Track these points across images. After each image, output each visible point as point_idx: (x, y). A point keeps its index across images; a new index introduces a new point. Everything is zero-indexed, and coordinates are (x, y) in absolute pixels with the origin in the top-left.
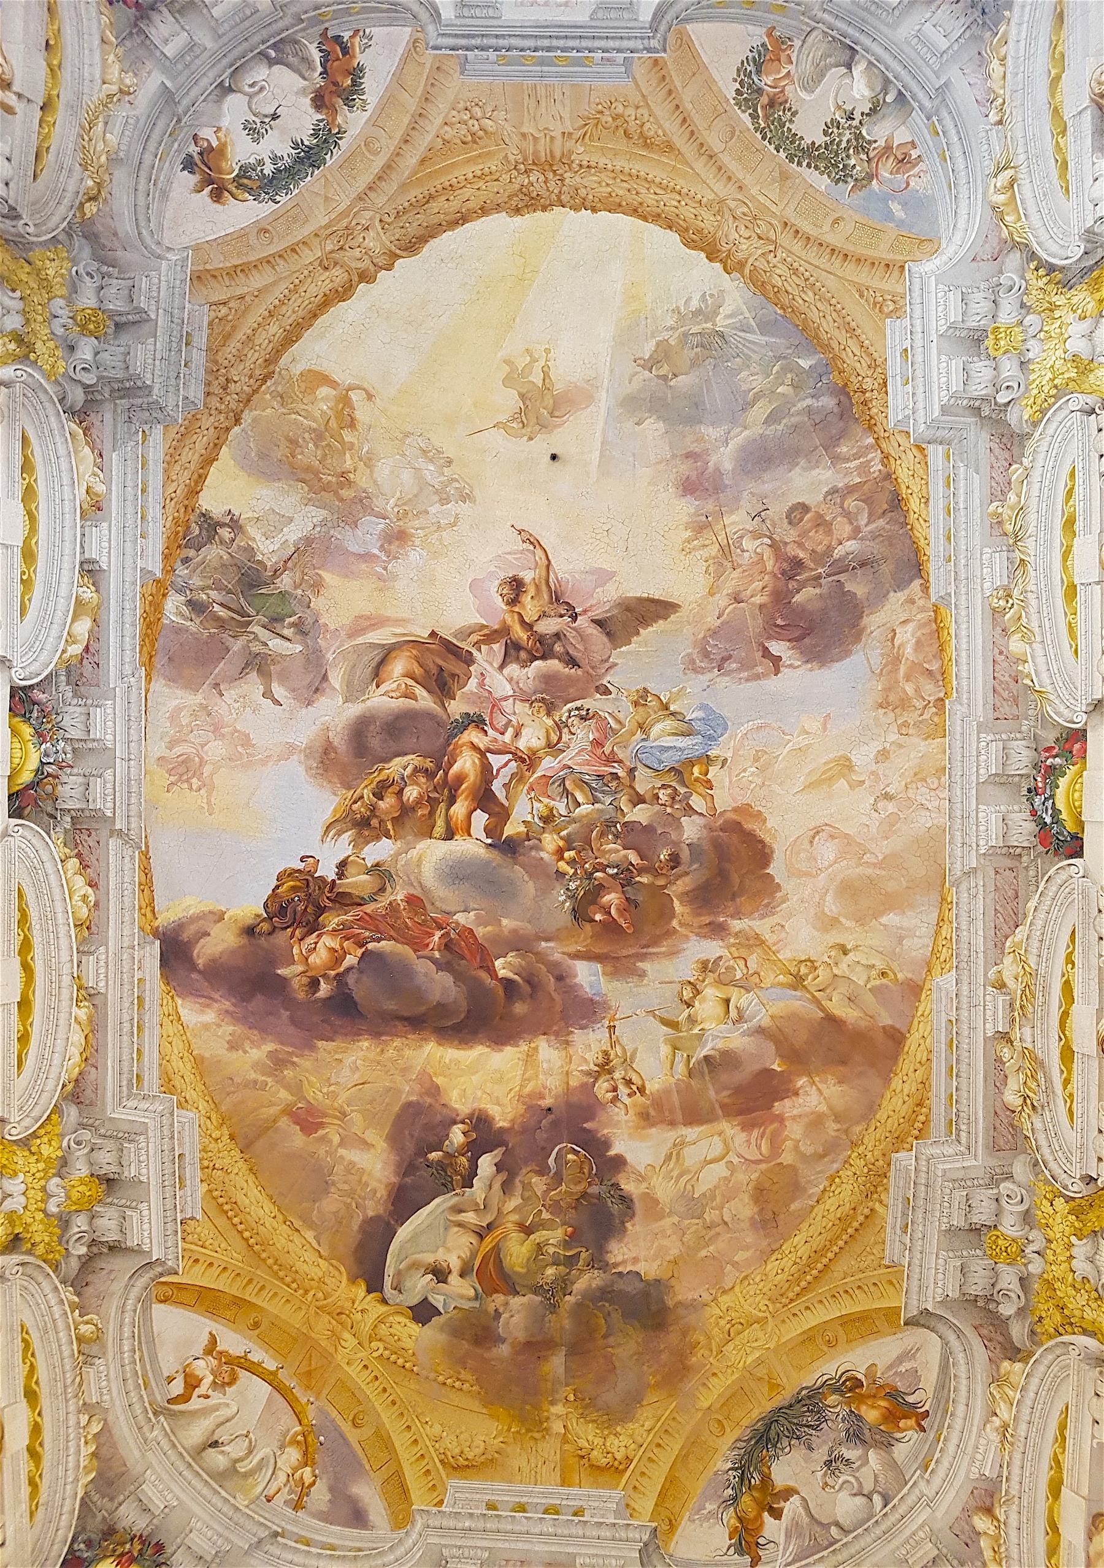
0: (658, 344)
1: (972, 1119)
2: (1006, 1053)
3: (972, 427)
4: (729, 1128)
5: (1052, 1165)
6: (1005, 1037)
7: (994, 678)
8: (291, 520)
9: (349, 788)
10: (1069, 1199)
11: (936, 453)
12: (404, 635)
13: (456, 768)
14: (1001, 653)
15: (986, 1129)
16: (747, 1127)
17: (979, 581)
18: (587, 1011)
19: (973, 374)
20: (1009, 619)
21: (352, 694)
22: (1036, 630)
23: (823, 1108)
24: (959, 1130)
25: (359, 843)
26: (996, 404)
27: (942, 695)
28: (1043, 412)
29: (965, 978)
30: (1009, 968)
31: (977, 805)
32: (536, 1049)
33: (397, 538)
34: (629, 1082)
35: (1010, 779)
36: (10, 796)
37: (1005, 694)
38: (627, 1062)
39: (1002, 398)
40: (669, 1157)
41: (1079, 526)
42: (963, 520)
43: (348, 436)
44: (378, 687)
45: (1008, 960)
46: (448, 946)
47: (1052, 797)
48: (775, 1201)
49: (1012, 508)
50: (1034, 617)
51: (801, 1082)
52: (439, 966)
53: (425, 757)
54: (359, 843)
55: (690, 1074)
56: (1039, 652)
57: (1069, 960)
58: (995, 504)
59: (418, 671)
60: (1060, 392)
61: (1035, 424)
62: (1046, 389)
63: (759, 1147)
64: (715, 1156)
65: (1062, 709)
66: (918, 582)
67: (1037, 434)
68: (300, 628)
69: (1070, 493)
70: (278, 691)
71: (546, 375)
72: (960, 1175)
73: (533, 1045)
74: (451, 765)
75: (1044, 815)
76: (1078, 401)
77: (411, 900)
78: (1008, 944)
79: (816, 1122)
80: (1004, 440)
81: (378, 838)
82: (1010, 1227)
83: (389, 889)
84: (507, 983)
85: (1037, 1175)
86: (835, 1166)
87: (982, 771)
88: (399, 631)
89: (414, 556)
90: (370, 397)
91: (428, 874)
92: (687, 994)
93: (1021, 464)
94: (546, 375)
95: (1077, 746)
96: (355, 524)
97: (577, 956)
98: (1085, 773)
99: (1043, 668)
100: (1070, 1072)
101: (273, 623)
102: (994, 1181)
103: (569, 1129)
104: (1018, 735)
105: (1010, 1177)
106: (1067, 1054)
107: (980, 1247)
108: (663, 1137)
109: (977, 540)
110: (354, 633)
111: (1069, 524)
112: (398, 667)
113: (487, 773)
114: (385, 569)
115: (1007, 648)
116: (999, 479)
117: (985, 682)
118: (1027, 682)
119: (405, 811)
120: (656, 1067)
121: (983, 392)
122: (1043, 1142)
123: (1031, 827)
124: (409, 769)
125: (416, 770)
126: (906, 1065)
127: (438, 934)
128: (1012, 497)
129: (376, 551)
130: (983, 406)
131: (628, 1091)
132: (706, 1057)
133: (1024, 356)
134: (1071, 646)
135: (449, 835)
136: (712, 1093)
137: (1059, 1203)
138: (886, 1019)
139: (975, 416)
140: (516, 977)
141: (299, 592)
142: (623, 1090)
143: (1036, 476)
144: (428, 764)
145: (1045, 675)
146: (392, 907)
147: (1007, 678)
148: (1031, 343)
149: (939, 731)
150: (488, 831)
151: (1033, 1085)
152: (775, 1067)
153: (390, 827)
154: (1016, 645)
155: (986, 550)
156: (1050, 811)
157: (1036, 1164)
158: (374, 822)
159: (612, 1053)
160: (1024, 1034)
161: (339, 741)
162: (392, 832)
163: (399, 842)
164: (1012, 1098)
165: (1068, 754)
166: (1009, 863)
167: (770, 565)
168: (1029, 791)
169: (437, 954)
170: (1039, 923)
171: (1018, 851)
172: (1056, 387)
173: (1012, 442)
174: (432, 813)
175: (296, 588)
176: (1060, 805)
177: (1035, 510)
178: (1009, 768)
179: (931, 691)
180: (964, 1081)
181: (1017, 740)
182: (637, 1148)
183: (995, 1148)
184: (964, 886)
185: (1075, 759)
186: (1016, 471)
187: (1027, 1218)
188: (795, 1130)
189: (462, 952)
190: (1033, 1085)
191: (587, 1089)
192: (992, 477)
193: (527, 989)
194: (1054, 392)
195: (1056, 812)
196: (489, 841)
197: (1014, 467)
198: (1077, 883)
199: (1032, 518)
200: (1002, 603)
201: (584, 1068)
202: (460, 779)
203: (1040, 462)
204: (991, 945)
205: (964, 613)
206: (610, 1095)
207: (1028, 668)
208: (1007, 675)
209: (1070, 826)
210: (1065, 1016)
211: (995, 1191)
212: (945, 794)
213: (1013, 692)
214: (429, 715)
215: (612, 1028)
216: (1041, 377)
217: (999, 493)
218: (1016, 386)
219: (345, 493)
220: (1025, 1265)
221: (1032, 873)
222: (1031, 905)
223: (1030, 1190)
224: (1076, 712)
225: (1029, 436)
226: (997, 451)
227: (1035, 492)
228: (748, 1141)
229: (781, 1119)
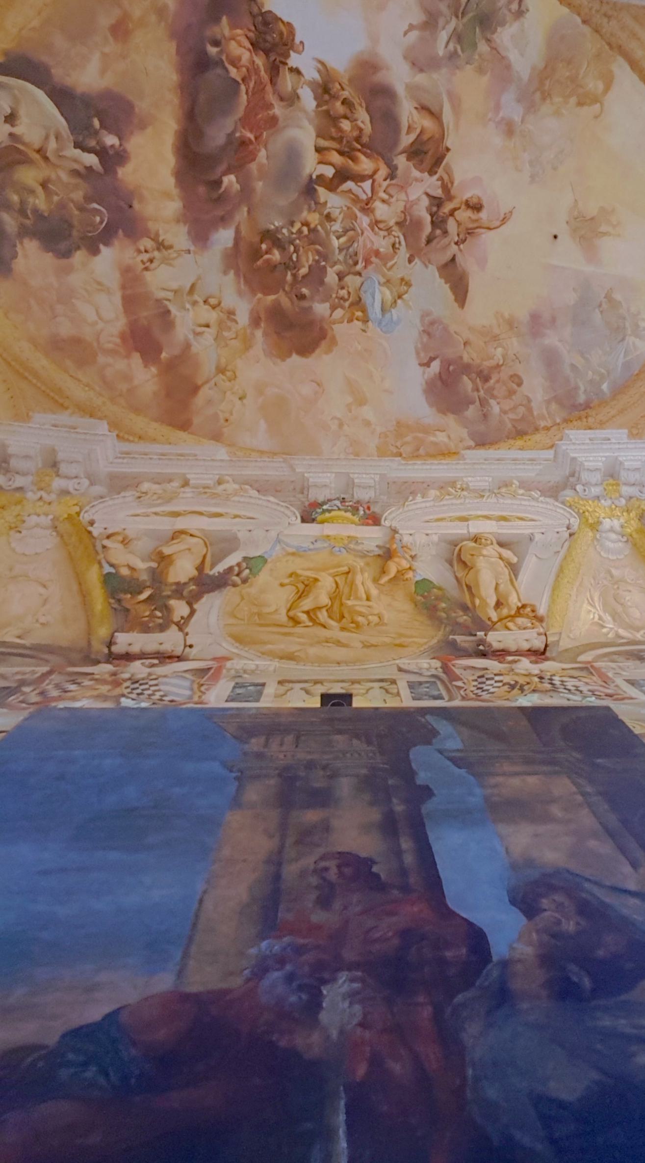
0: (620, 302)
4: (121, 323)
8: (522, 55)
9: (350, 81)
11: (550, 454)
12: (448, 129)
13: (362, 157)
16: (123, 336)
18: (201, 235)
21: (411, 89)
23: (136, 382)
25: (313, 85)
27: (404, 455)
32: (173, 200)
33: (509, 129)
34: (151, 261)
38: (166, 261)
40: (99, 283)
43: (573, 100)
44: (416, 108)
46: (244, 143)
48: (74, 350)
51: (154, 370)
52: (230, 136)
53: (370, 137)
54: (313, 85)
55: (158, 301)
59: (425, 137)
63: (109, 342)
64: (102, 313)
66: (472, 443)
68: (453, 56)
70: (414, 35)
71: (605, 234)
73: (176, 198)
74: (365, 154)
77: (273, 121)
79: (127, 378)
81: (316, 98)
83: (282, 104)
84: (218, 183)
86: (97, 388)
87: (356, 475)
88: (451, 127)
89: (497, 140)
90: (596, 117)
91: (293, 133)
92: (212, 301)
94: (605, 234)
96: (519, 101)
97: (238, 231)
99: (418, 506)
101: (458, 36)
103: (121, 219)
108: (113, 280)
110: (450, 94)
112: (427, 123)
113: (359, 178)
114: (490, 120)
118: (411, 498)
119: (333, 119)
120: (162, 279)
124: (362, 125)
125: (361, 130)
126: (166, 430)
127: (251, 136)
129: (501, 115)
131: (145, 260)
132: (169, 312)
135: (318, 150)
136: (145, 314)
138: (197, 421)
140: (222, 189)
141: (477, 57)
142: (145, 257)
144: (365, 139)
145: (414, 507)
146: (270, 106)
149: (382, 452)
150: (321, 177)
152: (164, 355)
153: (324, 108)
154: (433, 493)
155: (490, 479)
158: (326, 97)
159: (170, 251)
160: (188, 492)
161: (380, 77)
162: (320, 109)
163: (313, 114)
167: (485, 363)
169: (238, 135)
171: (306, 492)
174: (333, 139)
175: (480, 56)
179: (406, 450)
182: (107, 262)
188: (120, 365)
189: (240, 152)
191: (146, 233)
193: (215, 195)
196: (314, 177)
200: (459, 486)
201: (161, 232)
202: (354, 159)
205: (454, 467)
206: (142, 248)
207: (419, 498)
212: (342, 456)
213: (406, 491)
214: (396, 142)
215: (189, 252)
219: (538, 95)
221: (292, 499)
228: (112, 336)
229: (128, 356)
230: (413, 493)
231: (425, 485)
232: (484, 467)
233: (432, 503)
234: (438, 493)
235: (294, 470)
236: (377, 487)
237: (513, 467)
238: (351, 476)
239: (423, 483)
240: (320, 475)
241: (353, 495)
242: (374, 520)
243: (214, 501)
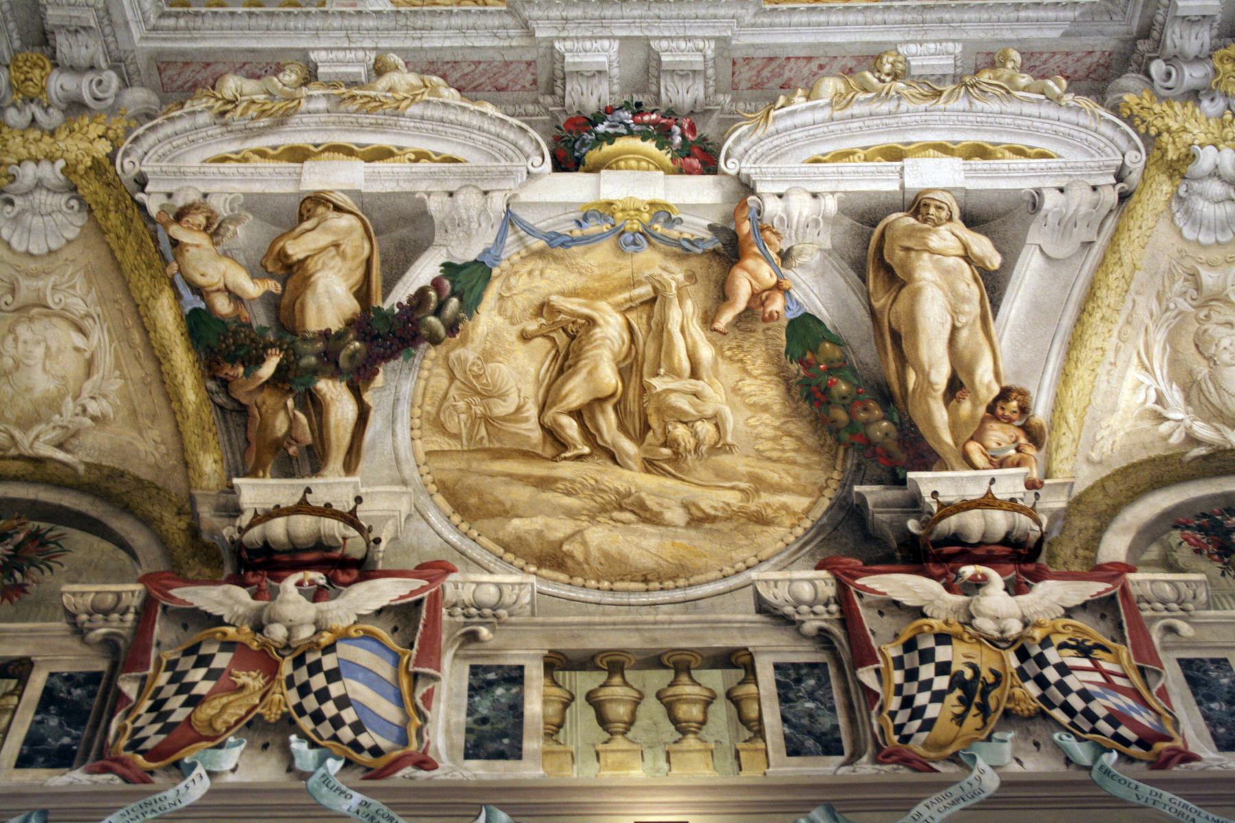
1: (196, 34)
2: (290, 77)
3: (1125, 28)
5: (152, 138)
6: (310, 76)
7: (788, 59)
10: (111, 157)
14: (821, 67)
15: (182, 53)
17: (919, 38)
19: (1196, 28)
20: (864, 77)
22: (848, 112)
24: (177, 15)
26: (1151, 59)
28: (1129, 120)
29: (384, 23)
30: (403, 80)
31: (621, 39)
35: (654, 80)
37: (766, 73)
39: (1157, 68)
41: (978, 163)
42: (1004, 16)
45: (413, 79)
47: (631, 133)
49: (1010, 81)
50: (865, 109)
56: (820, 115)
57: (420, 156)
58: (1018, 58)
60: (1151, 141)
61: (1115, 110)
62: (1159, 123)
65: (745, 144)
67: (1101, 111)
69: (1020, 152)
72: (116, 17)
75: (606, 123)
76: (1136, 160)
78: (435, 79)
80: (1102, 70)
82: (60, 84)
85: (135, 117)
87: (664, 44)
93: (1067, 91)
95: (696, 163)
98: (661, 173)
99: (798, 120)
100: (276, 158)
102: (116, 64)
104: (711, 90)
105: (126, 83)
106: (298, 155)
107: (25, 44)
109: (975, 34)
111: (981, 152)
115: (829, 75)
116: (1051, 64)
117: (783, 46)
118: (782, 100)
121: (1169, 42)
122: (179, 126)
123: (592, 105)
128: (1025, 79)
130: (1151, 42)
133: (1207, 94)
134: (824, 155)
137: (103, 148)
139: (1138, 32)
143: (1051, 111)
145: (789, 122)
147: (787, 74)
148: (1220, 103)
151: (253, 112)
154: (830, 86)
155: (958, 48)
156: (611, 130)
157: (150, 117)
160: (316, 99)
164: (232, 85)
165: (686, 150)
166: (543, 79)
168: (639, 105)
170: (465, 118)
171: (559, 91)
172: (1159, 134)
173: (1096, 81)
176: (621, 144)
177: (1004, 108)
178: (668, 78)
180: (245, 22)
181: (706, 88)
183: (162, 62)
184: (508, 20)
185: (680, 160)
186: (1056, 86)
187: (75, 107)
190: (253, 112)
192: (1054, 54)
194: (1153, 131)
195: (610, 138)
197: (1064, 83)
198: (521, 166)
199: (995, 106)
200: (887, 68)
203: (1065, 115)
204: (432, 56)
205: (879, 17)
207: (799, 102)
208: (792, 75)
209: (593, 156)
210: (348, 151)
211: (103, 65)
213: (767, 81)
216: (1174, 116)
217: (1037, 64)
218: (1169, 84)
220: (14, 105)
221: (530, 108)
222: (489, 109)
223: (113, 110)
224: (740, 162)
225: (1101, 102)
226: (1088, 60)
227: (1028, 109)
230: (787, 87)
231: (814, 66)
232: (947, 16)
233: (826, 113)
234: (841, 86)
235: (531, 34)
236: (710, 72)
237: (1013, 15)
238: (653, 44)
239: (809, 59)
240: (588, 44)
241: (658, 94)
242: (702, 157)
243: (372, 118)
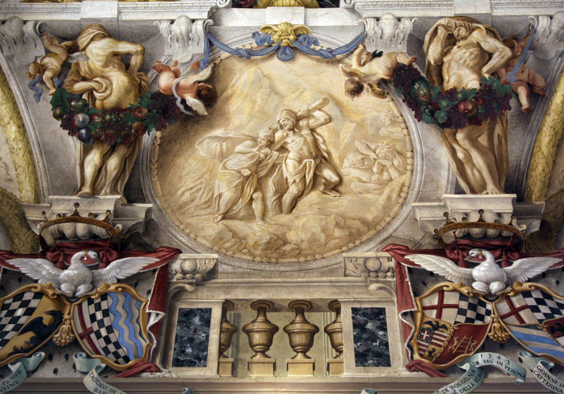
36: (322, 6)
